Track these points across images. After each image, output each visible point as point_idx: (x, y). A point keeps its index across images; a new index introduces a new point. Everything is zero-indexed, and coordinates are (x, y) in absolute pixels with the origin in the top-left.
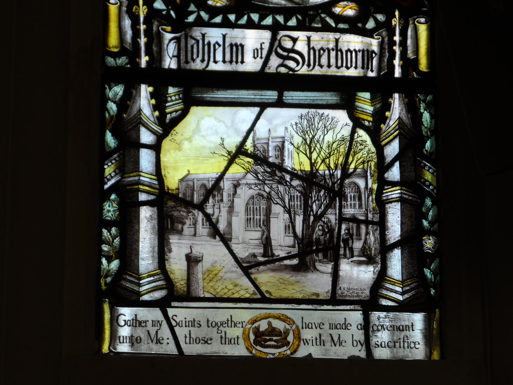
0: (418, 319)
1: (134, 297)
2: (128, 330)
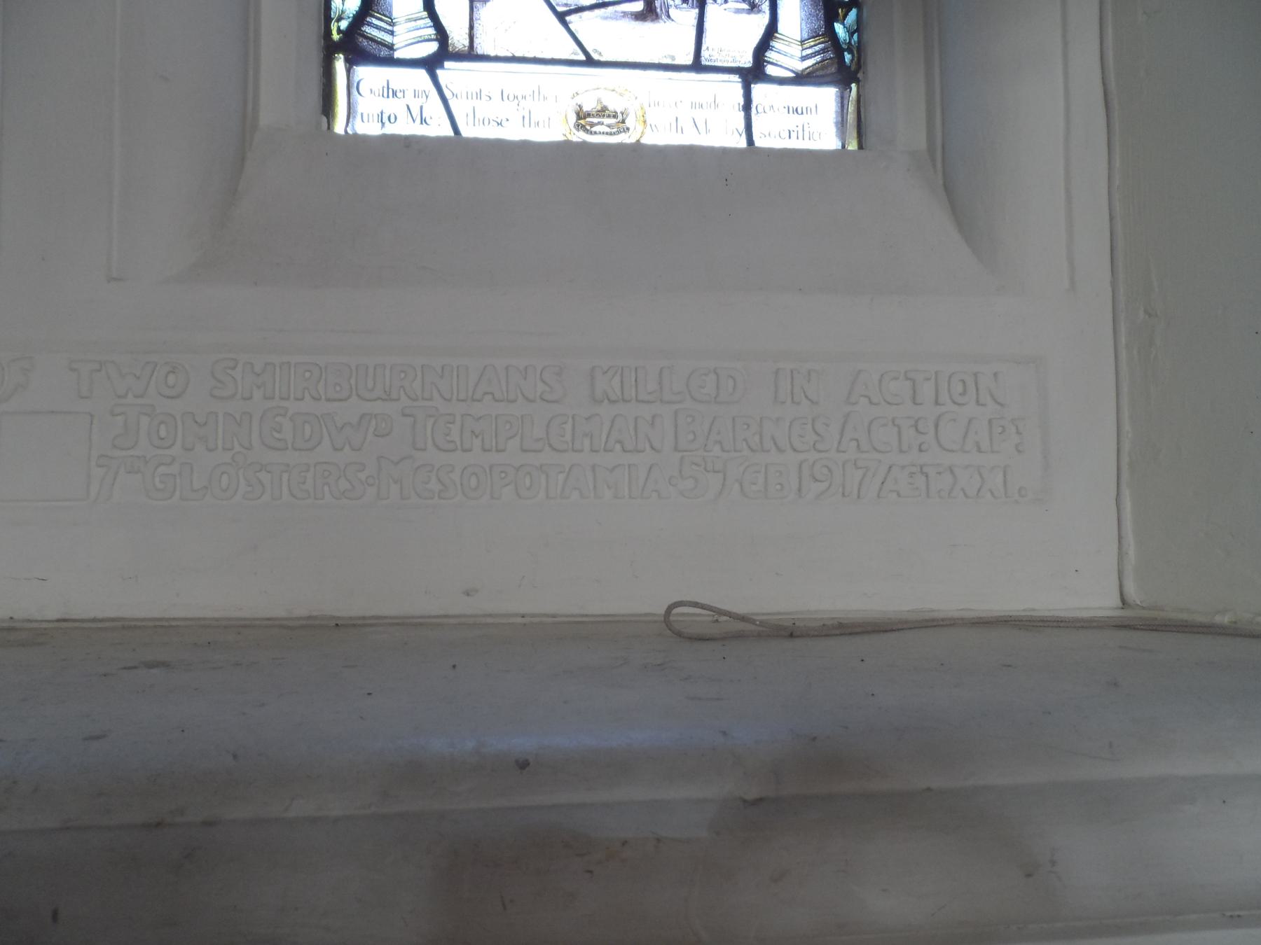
0: (826, 97)
1: (384, 52)
2: (377, 103)
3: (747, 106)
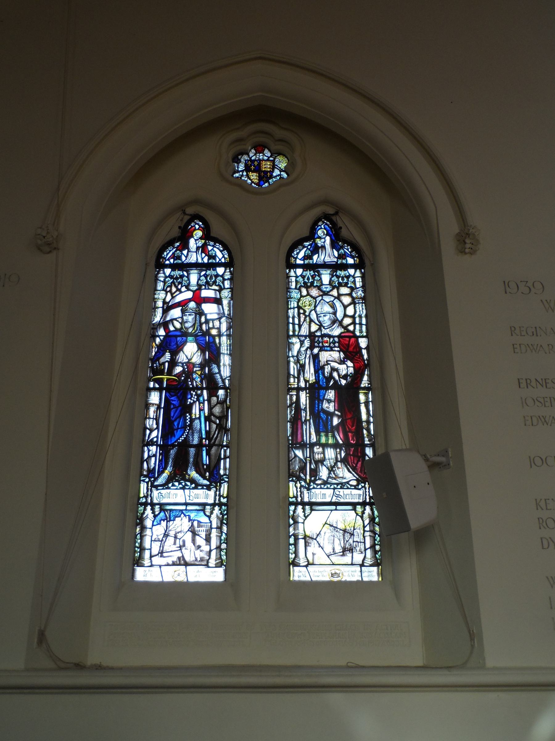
0: (375, 569)
3: (361, 572)
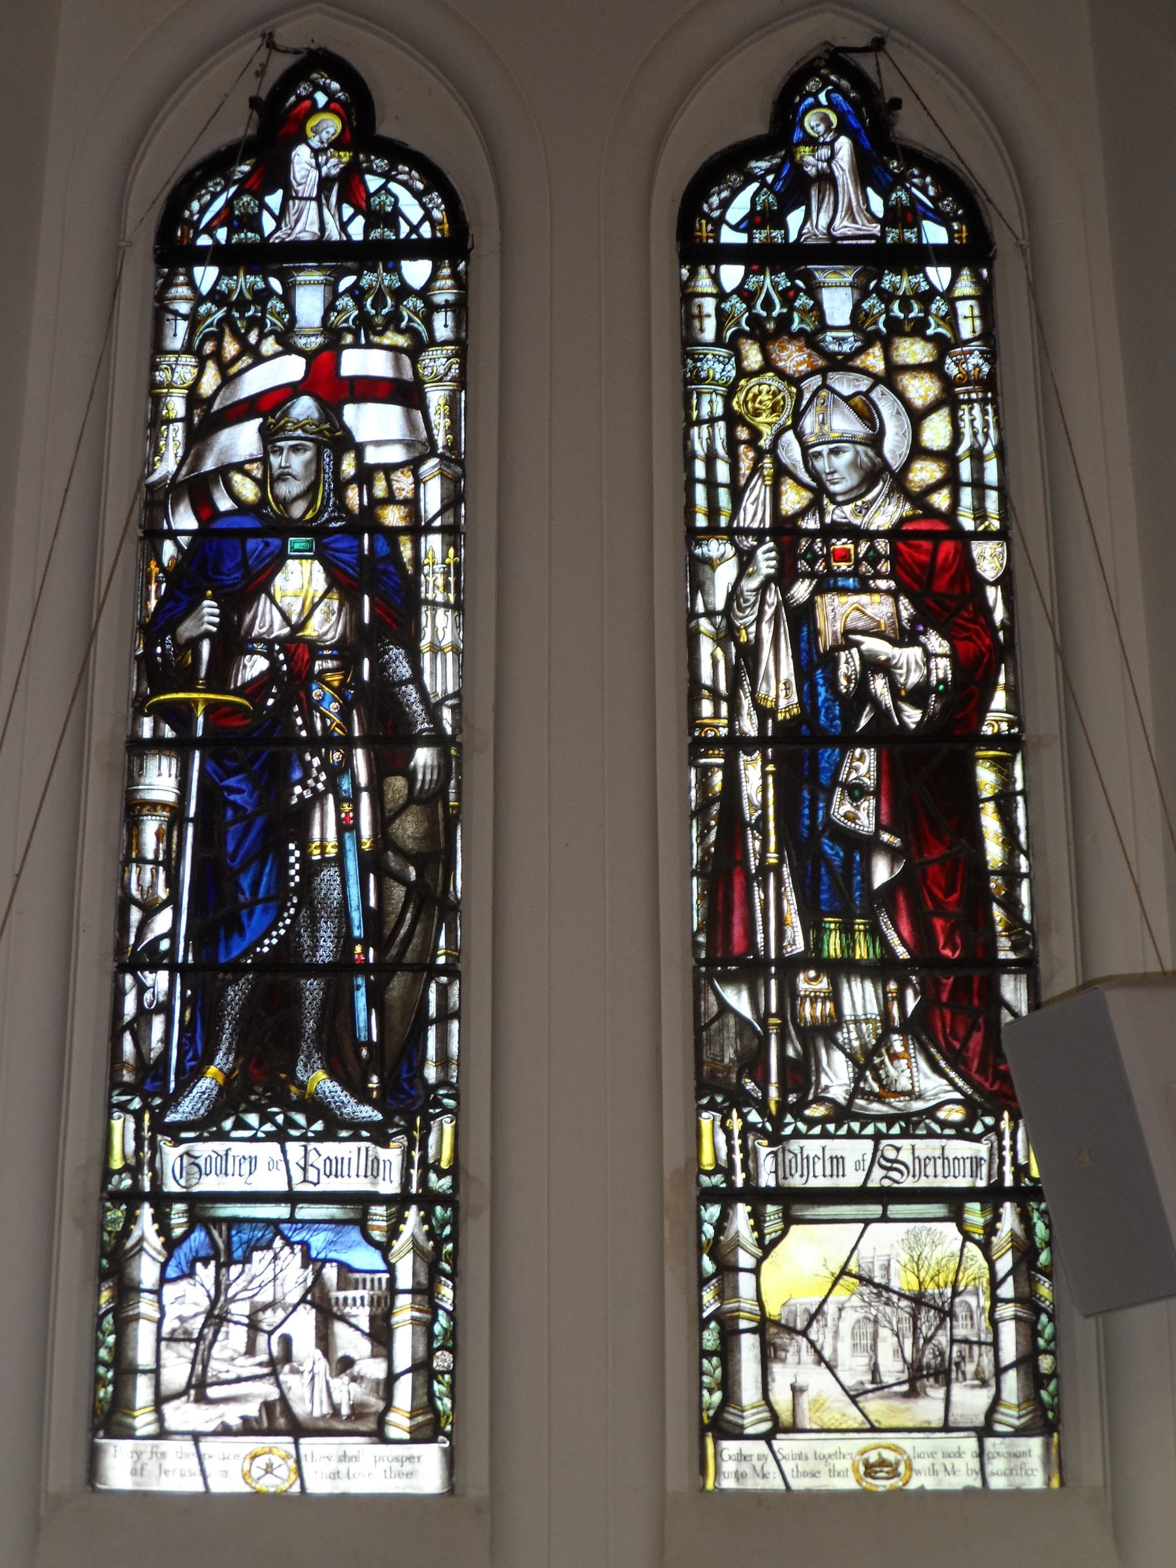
0: (1035, 1445)
1: (737, 1431)
2: (737, 1466)
